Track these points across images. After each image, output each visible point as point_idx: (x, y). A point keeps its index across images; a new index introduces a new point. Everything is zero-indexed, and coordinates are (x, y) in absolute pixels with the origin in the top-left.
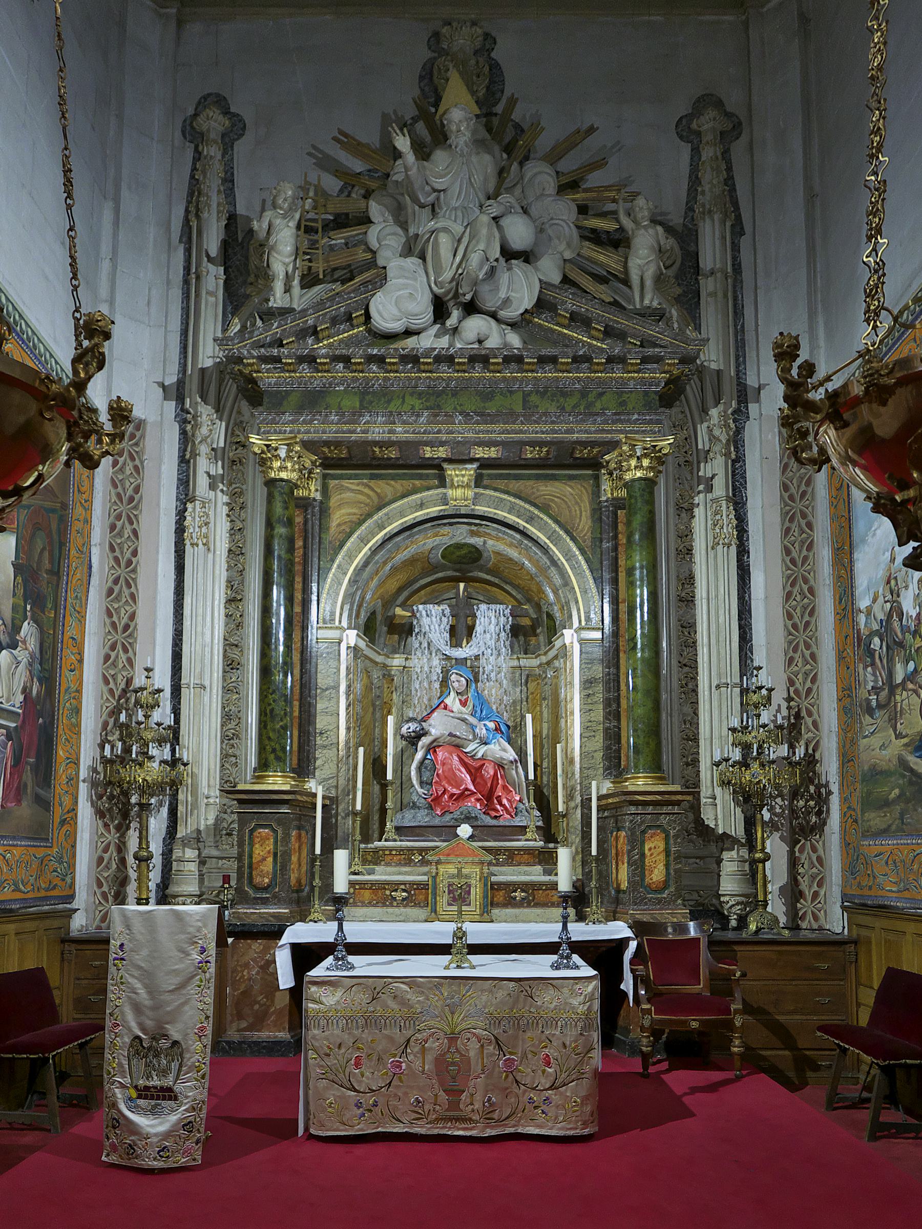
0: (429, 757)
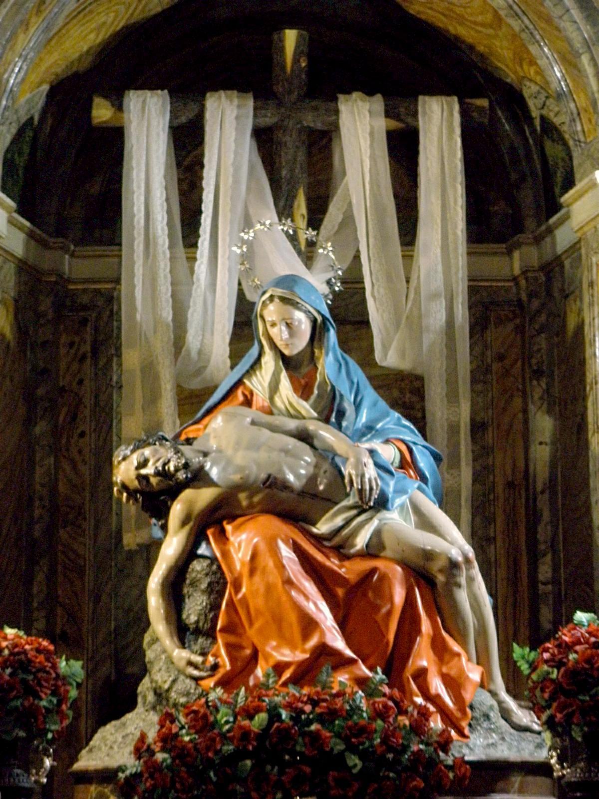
0: (203, 550)
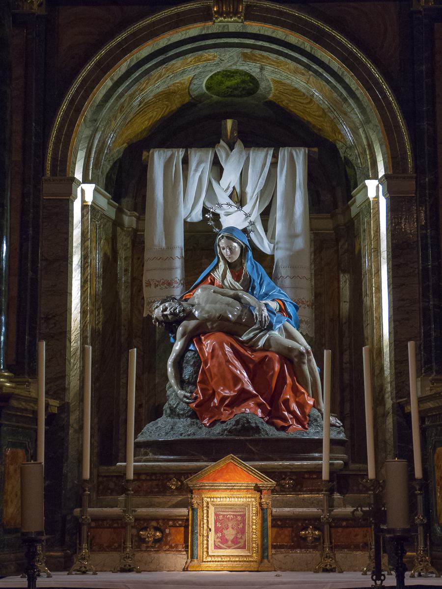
0: (191, 348)
